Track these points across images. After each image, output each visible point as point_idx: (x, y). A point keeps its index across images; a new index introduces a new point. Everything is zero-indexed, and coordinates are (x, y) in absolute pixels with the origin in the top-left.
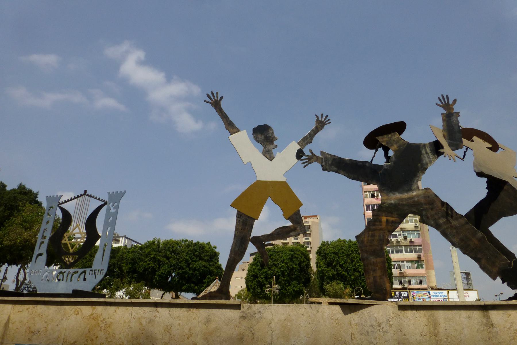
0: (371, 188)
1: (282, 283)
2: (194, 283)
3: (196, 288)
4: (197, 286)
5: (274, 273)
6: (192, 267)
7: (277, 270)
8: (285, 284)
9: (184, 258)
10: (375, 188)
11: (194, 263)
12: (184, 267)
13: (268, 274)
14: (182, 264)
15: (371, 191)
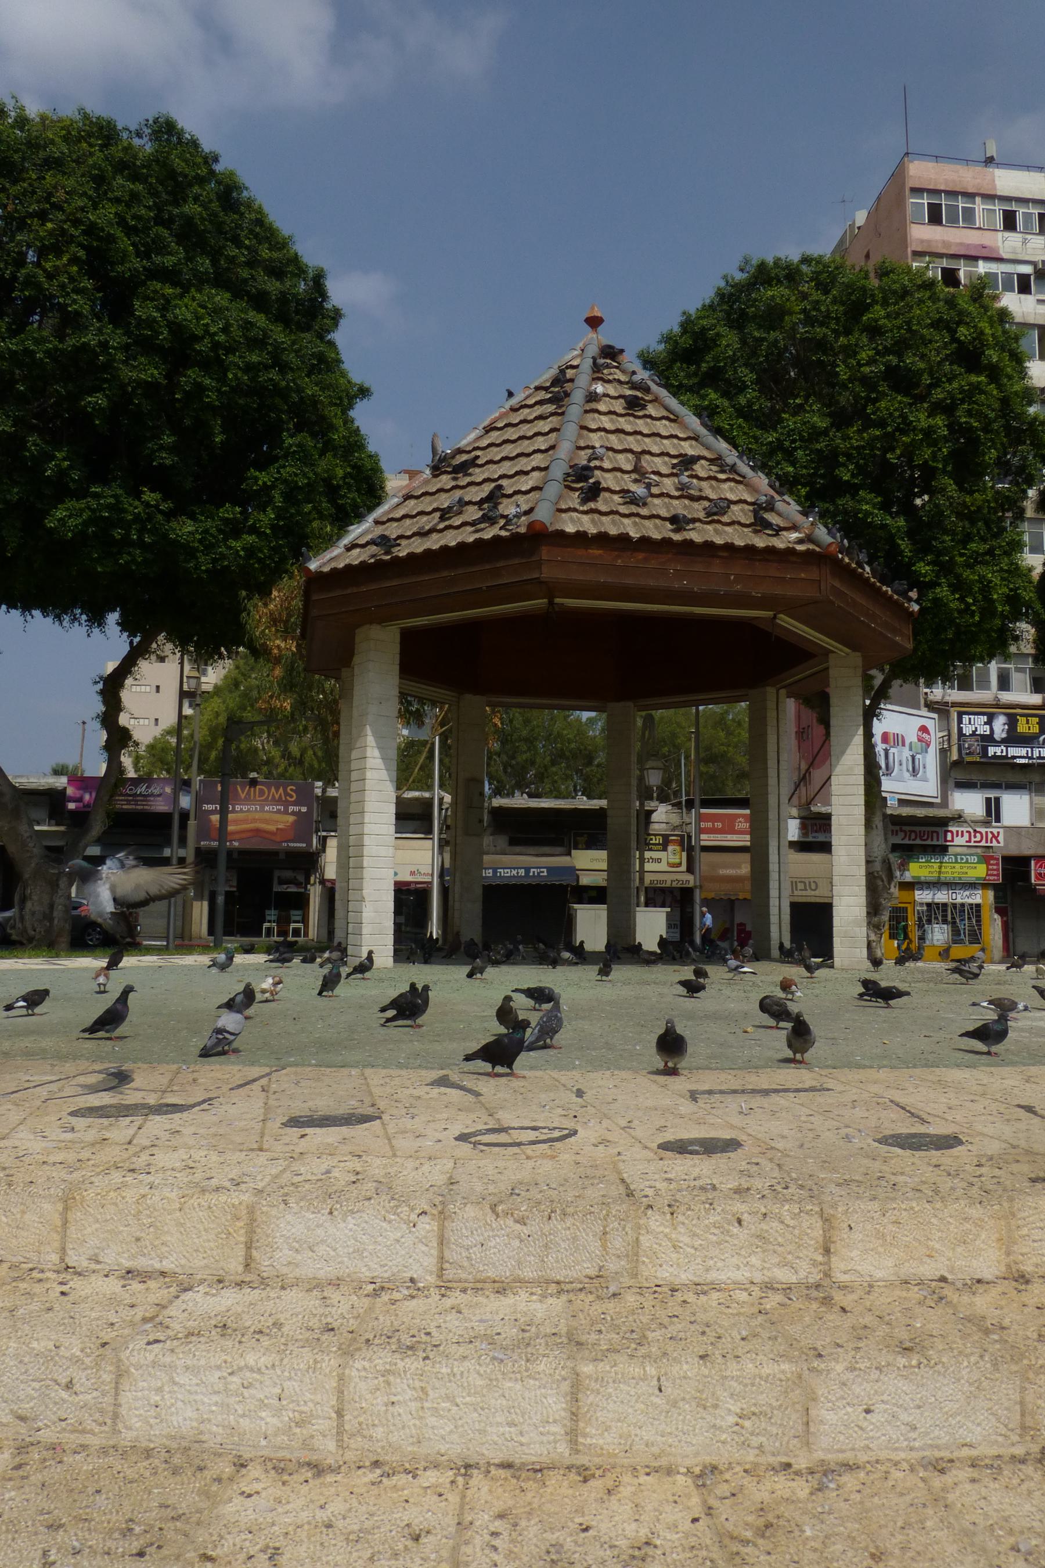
0: (944, 242)
1: (946, 532)
2: (160, 479)
3: (185, 529)
4: (192, 517)
5: (892, 449)
6: (151, 323)
7: (921, 418)
8: (967, 538)
9: (76, 223)
10: (961, 244)
11: (169, 291)
12: (80, 304)
13: (829, 460)
14: (50, 276)
15: (941, 256)
